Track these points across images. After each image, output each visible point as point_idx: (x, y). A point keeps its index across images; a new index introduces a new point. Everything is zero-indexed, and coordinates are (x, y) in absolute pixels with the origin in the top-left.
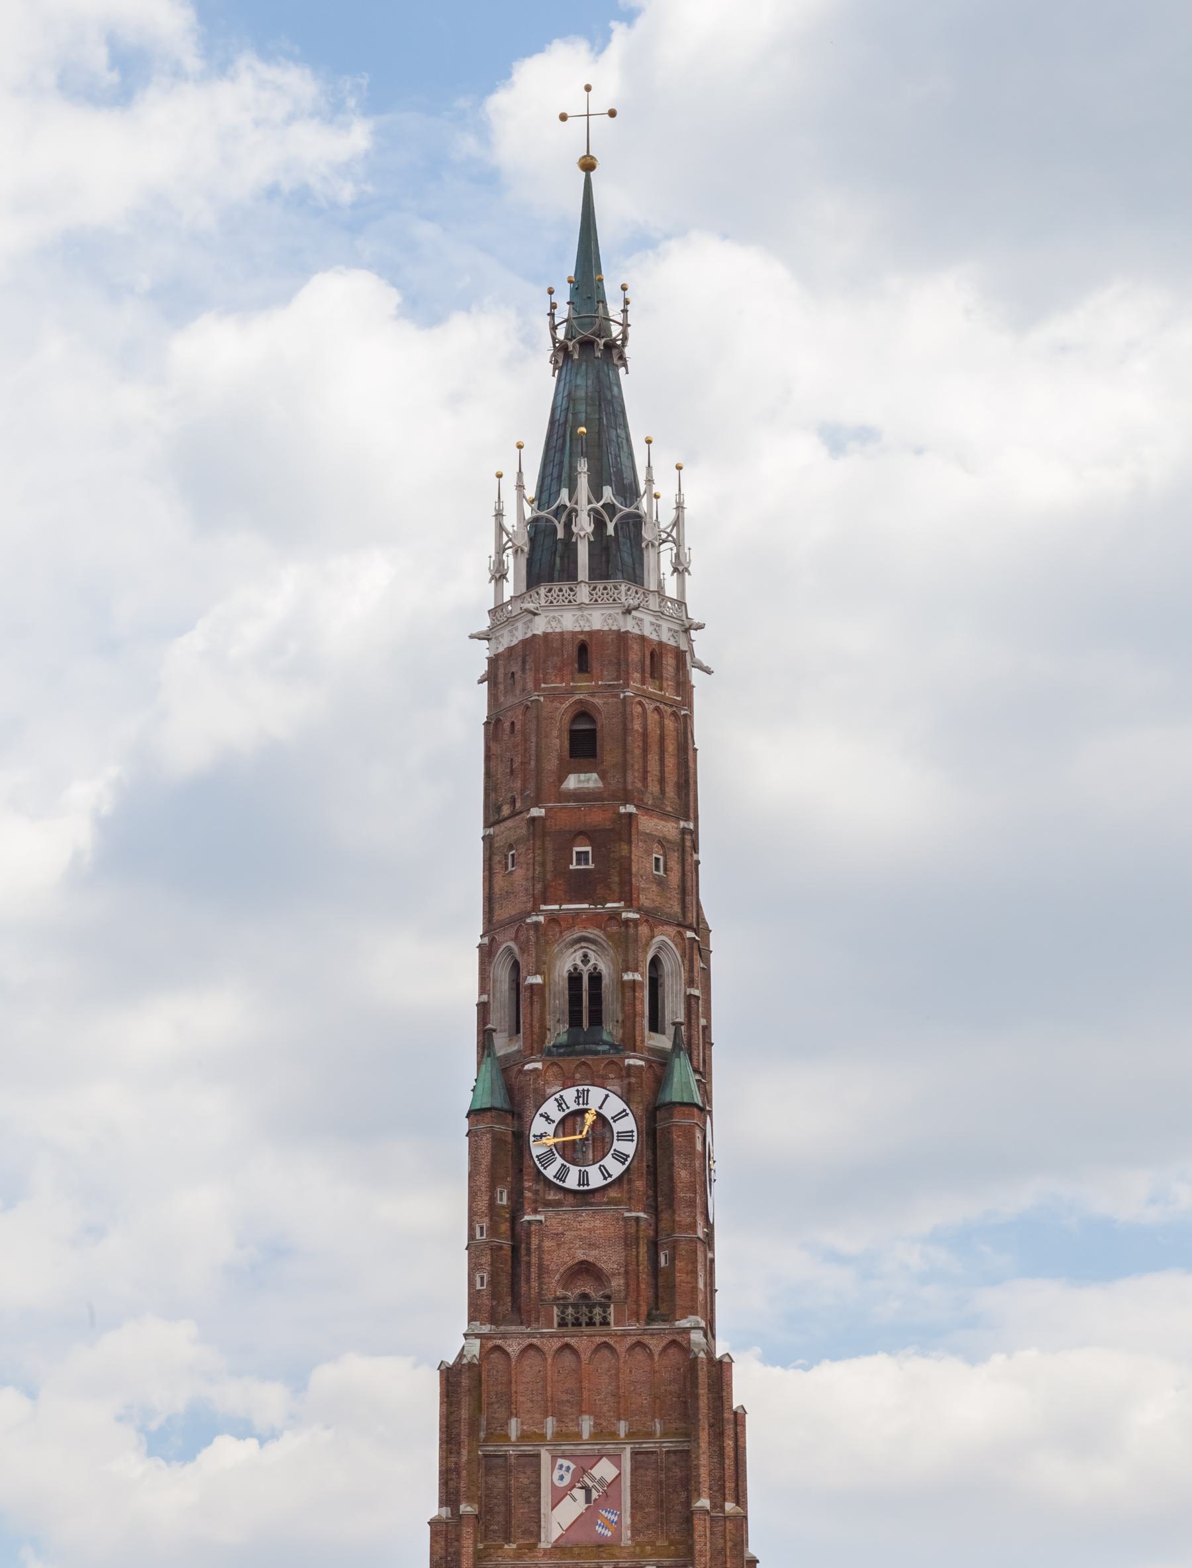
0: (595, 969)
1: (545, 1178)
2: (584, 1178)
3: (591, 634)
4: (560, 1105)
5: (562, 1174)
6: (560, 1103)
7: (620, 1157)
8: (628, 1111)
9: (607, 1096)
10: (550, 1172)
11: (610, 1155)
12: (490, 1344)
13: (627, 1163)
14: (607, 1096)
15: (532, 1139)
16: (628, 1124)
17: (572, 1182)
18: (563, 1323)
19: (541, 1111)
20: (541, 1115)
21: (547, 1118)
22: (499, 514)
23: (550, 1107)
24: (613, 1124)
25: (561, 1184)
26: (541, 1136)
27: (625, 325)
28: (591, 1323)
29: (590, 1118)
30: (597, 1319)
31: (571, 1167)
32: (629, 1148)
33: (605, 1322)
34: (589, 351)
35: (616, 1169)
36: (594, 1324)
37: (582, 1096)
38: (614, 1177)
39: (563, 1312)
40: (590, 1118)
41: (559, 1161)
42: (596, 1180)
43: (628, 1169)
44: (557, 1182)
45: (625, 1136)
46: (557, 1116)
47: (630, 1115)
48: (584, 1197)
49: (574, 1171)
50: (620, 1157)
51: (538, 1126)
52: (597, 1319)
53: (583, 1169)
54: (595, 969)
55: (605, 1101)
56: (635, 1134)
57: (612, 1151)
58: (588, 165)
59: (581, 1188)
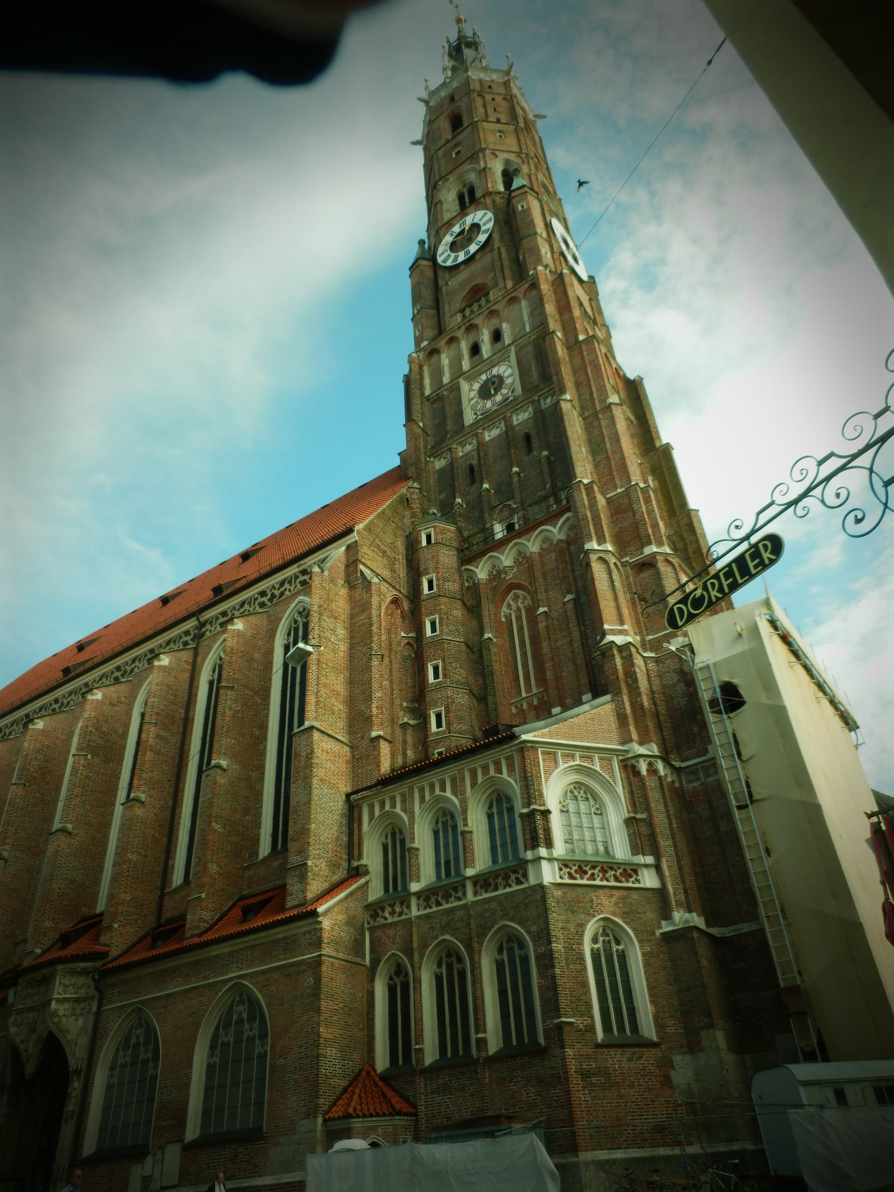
18: (464, 316)
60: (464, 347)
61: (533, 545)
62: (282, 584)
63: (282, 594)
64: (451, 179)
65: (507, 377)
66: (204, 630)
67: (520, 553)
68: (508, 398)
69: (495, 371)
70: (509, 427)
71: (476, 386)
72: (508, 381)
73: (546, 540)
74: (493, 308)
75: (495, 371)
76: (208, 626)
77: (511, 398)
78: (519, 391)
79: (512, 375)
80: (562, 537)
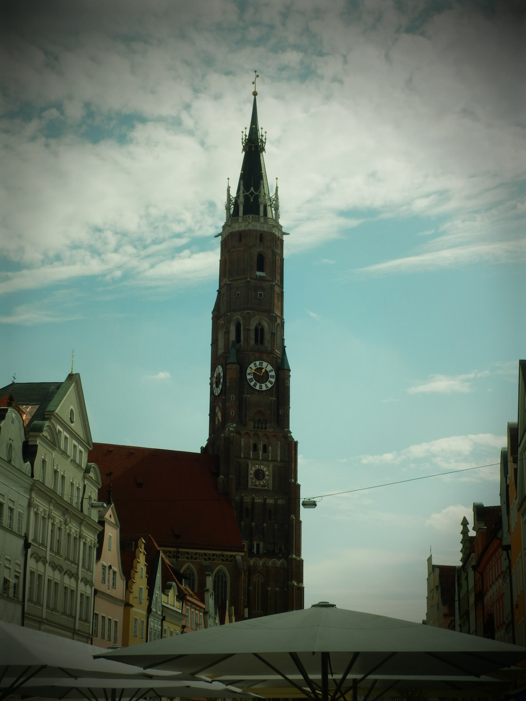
2: (261, 387)
3: (264, 231)
6: (255, 364)
7: (271, 382)
10: (252, 384)
16: (273, 373)
17: (257, 388)
18: (254, 427)
19: (250, 366)
22: (228, 191)
23: (252, 365)
27: (265, 143)
28: (262, 428)
29: (263, 371)
30: (264, 427)
32: (273, 380)
33: (266, 428)
34: (253, 148)
35: (270, 386)
37: (261, 364)
40: (263, 371)
41: (254, 381)
42: (264, 388)
45: (272, 377)
48: (261, 392)
49: (258, 385)
50: (271, 382)
52: (264, 427)
55: (267, 367)
58: (255, 94)
60: (252, 442)
61: (270, 563)
62: (214, 555)
63: (214, 560)
64: (257, 316)
65: (267, 475)
66: (178, 555)
67: (264, 562)
68: (265, 486)
69: (262, 467)
70: (265, 503)
71: (254, 469)
72: (267, 478)
73: (273, 563)
74: (267, 433)
75: (262, 467)
76: (180, 555)
77: (266, 488)
78: (271, 488)
79: (267, 475)
80: (279, 566)
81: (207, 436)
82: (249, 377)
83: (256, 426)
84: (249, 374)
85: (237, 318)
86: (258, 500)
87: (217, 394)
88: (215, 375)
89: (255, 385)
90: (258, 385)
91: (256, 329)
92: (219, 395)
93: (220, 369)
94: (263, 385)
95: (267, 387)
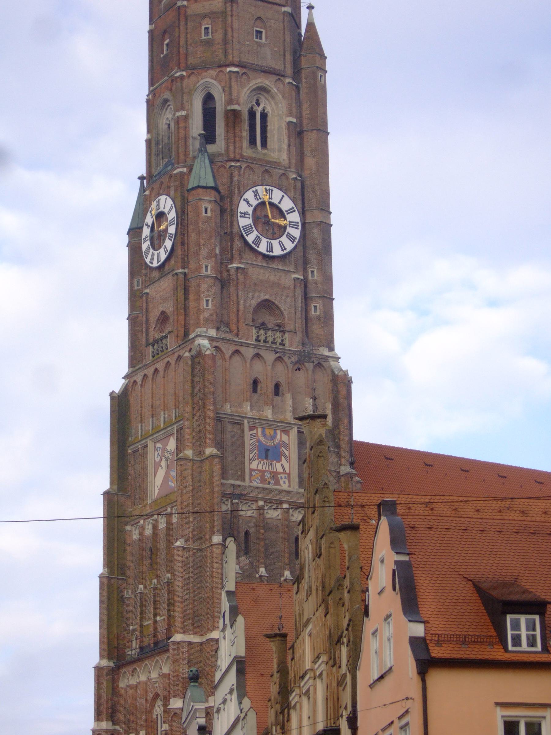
0: (264, 110)
1: (246, 243)
4: (255, 196)
5: (257, 241)
6: (256, 194)
7: (291, 238)
8: (295, 209)
9: (283, 196)
10: (250, 239)
11: (285, 236)
12: (215, 344)
13: (295, 243)
14: (283, 196)
15: (239, 214)
16: (295, 217)
17: (263, 248)
18: (258, 340)
19: (244, 197)
20: (244, 200)
21: (248, 203)
23: (249, 195)
24: (286, 215)
25: (256, 248)
26: (245, 214)
31: (263, 238)
32: (296, 233)
33: (282, 344)
35: (289, 246)
36: (276, 343)
38: (288, 250)
39: (258, 332)
41: (255, 233)
42: (277, 251)
43: (296, 246)
44: (254, 246)
45: (293, 225)
46: (254, 203)
47: (297, 211)
49: (264, 241)
50: (291, 238)
51: (243, 207)
53: (269, 241)
54: (264, 110)
56: (300, 224)
57: (286, 233)
59: (268, 253)
81: (125, 369)
82: (243, 222)
83: (262, 338)
84: (244, 215)
85: (207, 86)
86: (273, 514)
87: (155, 264)
88: (149, 220)
89: (257, 241)
90: (264, 241)
91: (252, 114)
92: (161, 267)
93: (166, 203)
94: (275, 243)
95: (283, 249)
